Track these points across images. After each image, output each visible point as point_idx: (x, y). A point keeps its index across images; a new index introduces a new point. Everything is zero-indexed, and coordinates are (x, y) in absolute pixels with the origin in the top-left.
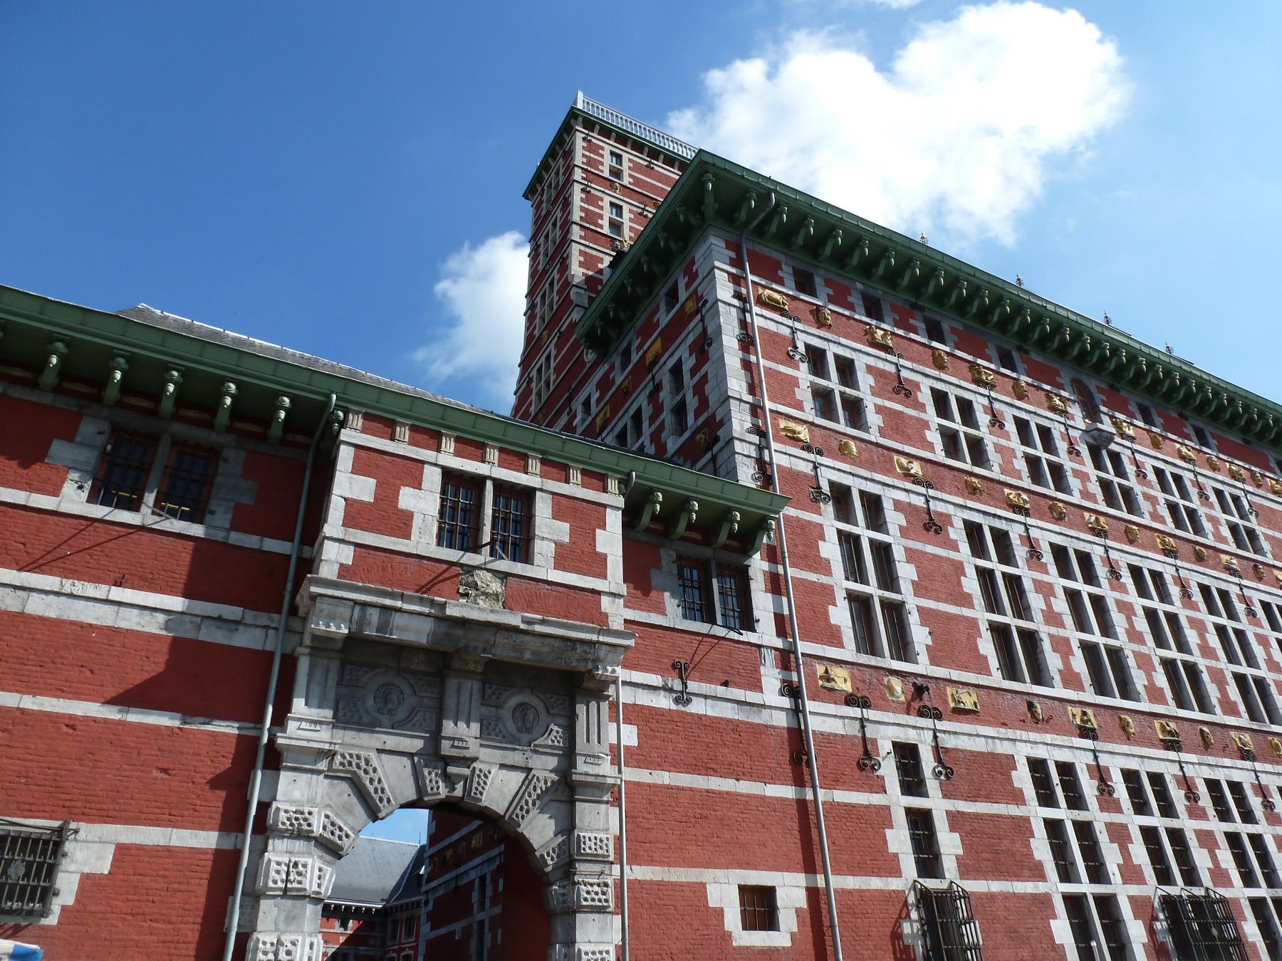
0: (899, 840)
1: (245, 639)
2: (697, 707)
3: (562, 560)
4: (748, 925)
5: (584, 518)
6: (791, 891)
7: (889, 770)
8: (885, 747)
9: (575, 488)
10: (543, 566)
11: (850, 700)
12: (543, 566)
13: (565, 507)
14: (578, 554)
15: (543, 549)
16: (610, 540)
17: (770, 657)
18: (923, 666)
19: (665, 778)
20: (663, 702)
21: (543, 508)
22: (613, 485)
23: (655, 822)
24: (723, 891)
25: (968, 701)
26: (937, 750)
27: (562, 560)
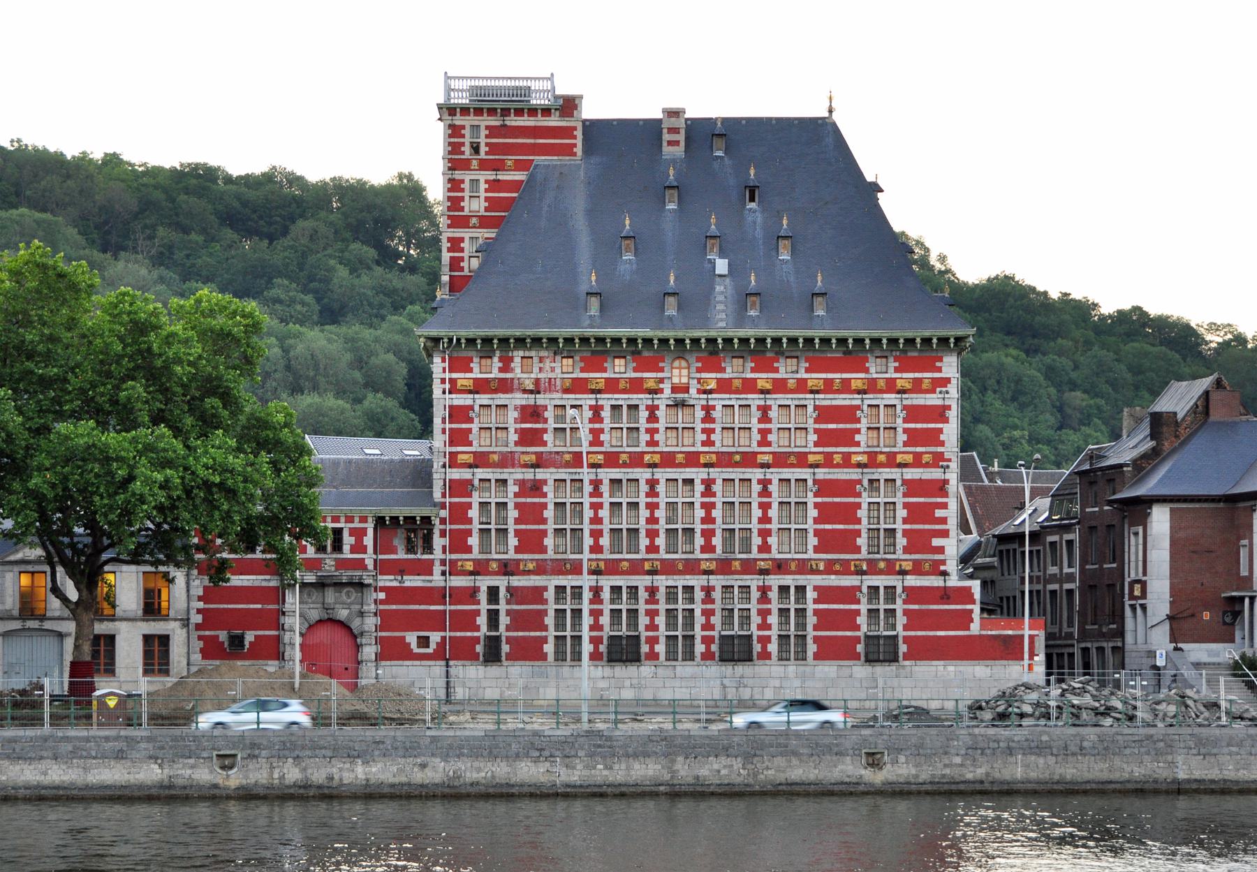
0: (482, 621)
1: (273, 584)
2: (407, 584)
3: (353, 551)
4: (419, 647)
5: (359, 534)
6: (435, 637)
7: (483, 596)
8: (484, 589)
9: (356, 525)
10: (347, 554)
11: (471, 573)
12: (347, 554)
13: (353, 532)
14: (359, 547)
15: (346, 548)
16: (369, 540)
17: (437, 563)
18: (511, 555)
19: (394, 607)
20: (395, 584)
21: (346, 534)
22: (370, 519)
23: (387, 621)
24: (412, 638)
25: (531, 566)
26: (508, 589)
27: (353, 551)
